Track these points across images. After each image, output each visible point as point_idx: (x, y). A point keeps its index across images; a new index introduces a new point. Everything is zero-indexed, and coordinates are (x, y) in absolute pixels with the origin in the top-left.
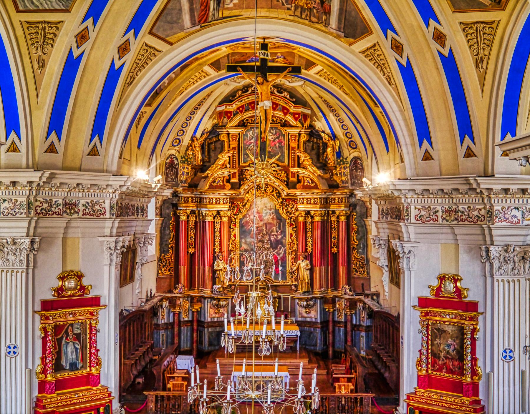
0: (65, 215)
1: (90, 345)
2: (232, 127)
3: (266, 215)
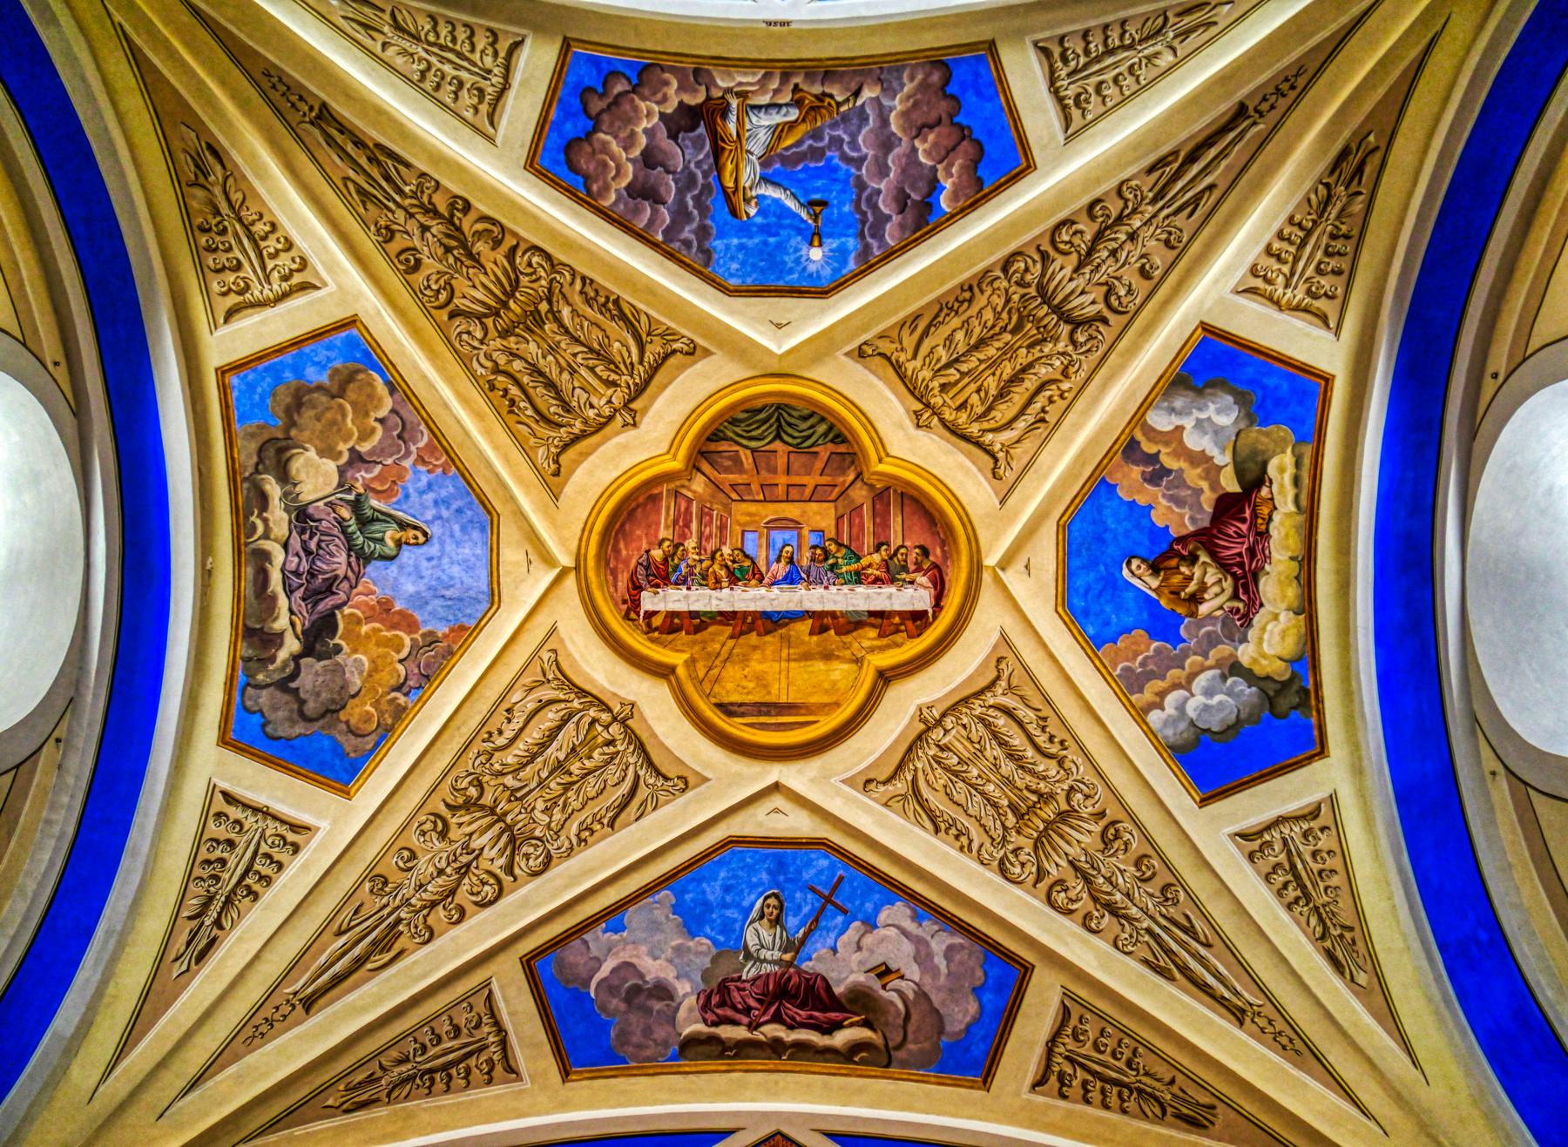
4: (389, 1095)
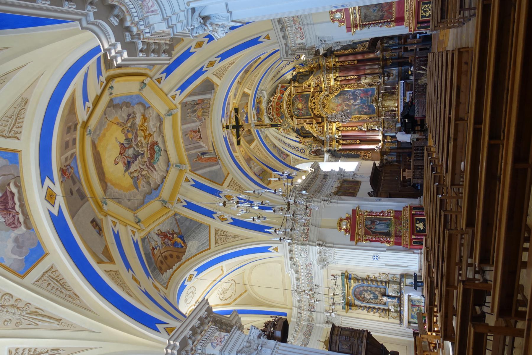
0: (309, 226)
1: (378, 216)
2: (293, 123)
4: (71, 291)
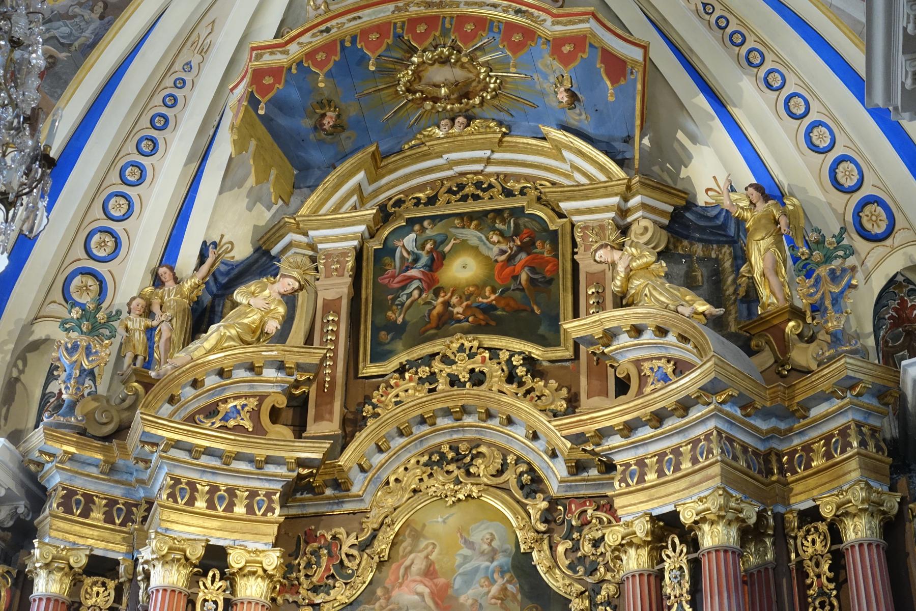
3: (468, 584)
